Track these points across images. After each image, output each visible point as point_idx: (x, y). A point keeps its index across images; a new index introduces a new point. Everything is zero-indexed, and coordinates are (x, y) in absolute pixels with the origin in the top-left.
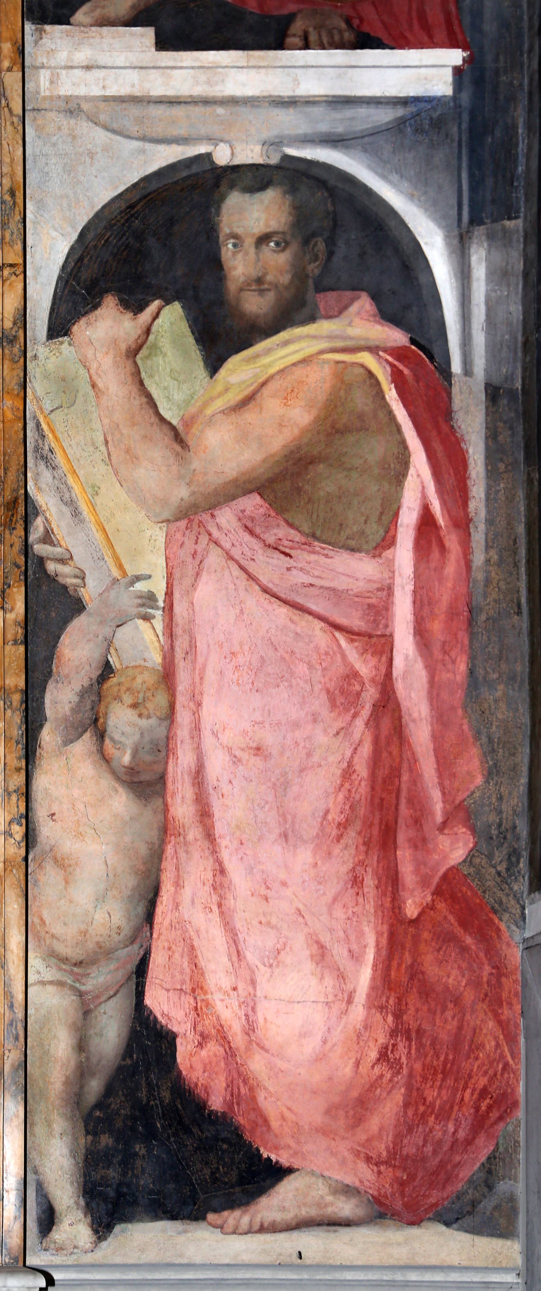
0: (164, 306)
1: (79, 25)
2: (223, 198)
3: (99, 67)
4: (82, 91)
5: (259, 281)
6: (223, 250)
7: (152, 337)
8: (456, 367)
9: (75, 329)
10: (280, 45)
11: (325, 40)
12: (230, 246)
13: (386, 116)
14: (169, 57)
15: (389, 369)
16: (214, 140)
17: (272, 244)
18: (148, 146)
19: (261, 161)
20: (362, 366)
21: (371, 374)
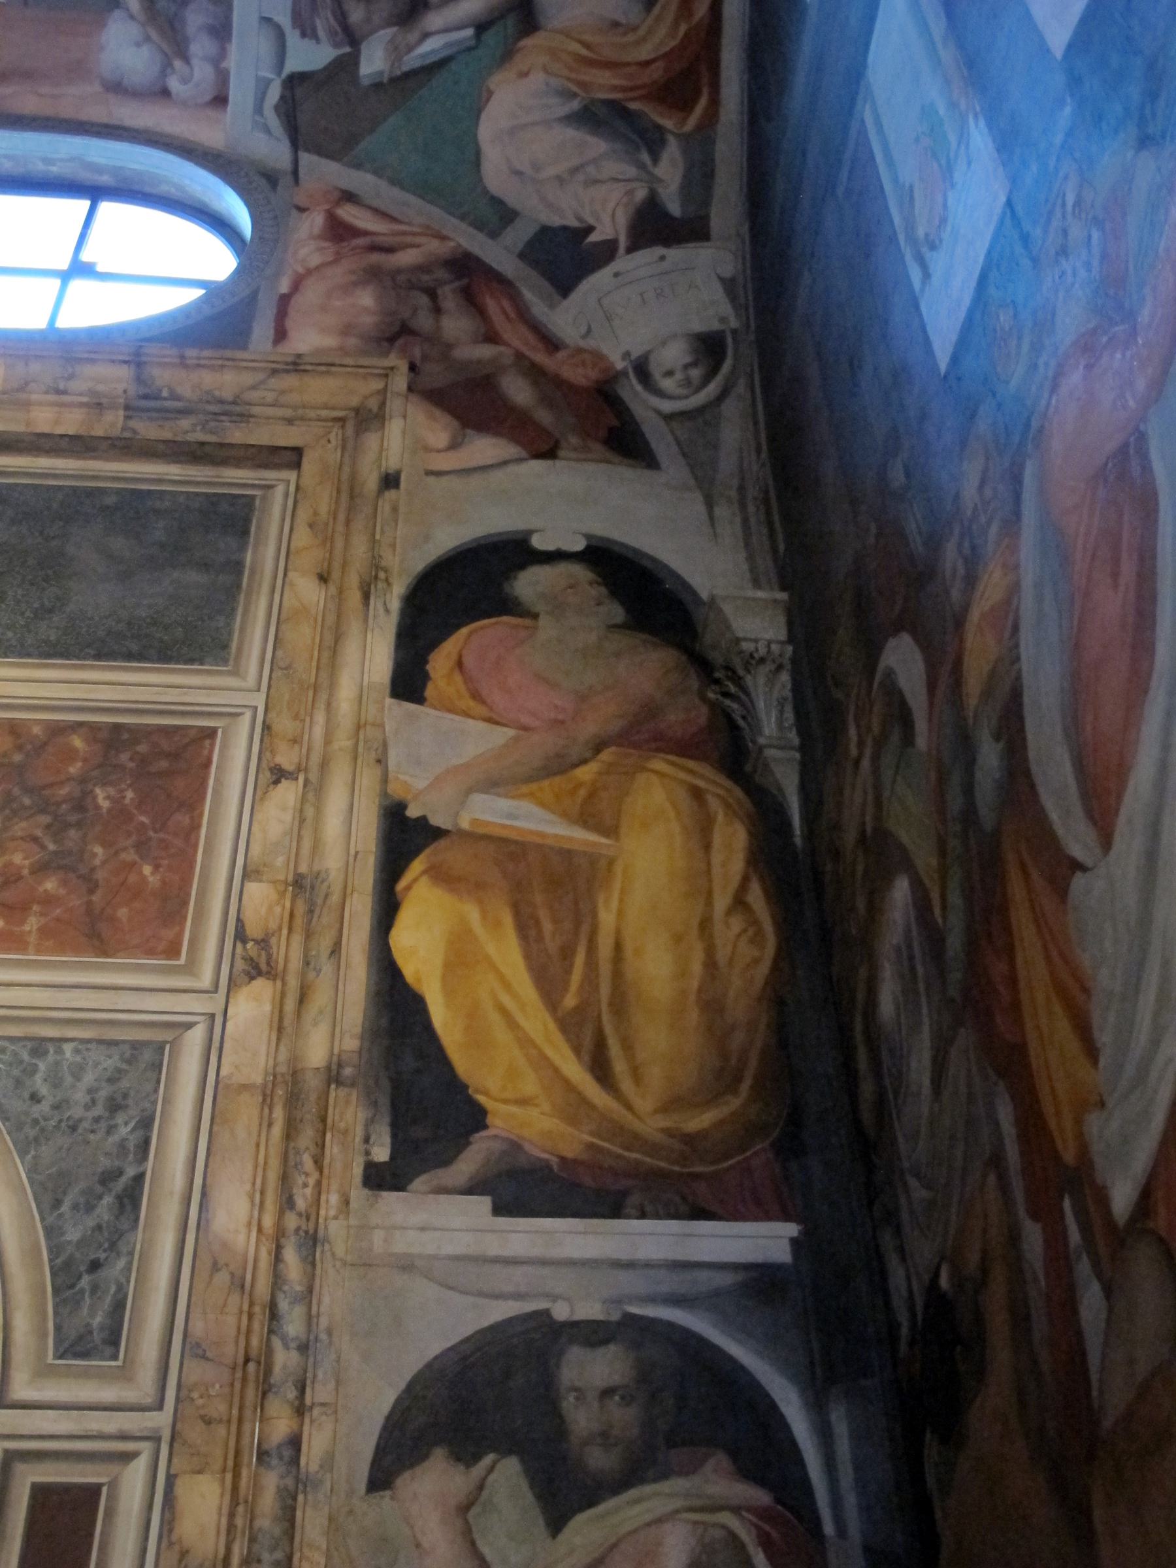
0: (498, 1460)
1: (416, 1192)
2: (561, 1353)
3: (435, 1229)
4: (415, 1250)
5: (604, 1434)
6: (564, 1404)
7: (485, 1494)
8: (829, 1528)
9: (399, 1482)
10: (616, 1212)
11: (661, 1212)
12: (571, 1399)
13: (726, 1279)
14: (504, 1222)
15: (754, 1531)
16: (555, 1298)
17: (617, 1398)
18: (486, 1301)
19: (601, 1317)
20: (724, 1527)
21: (733, 1536)
